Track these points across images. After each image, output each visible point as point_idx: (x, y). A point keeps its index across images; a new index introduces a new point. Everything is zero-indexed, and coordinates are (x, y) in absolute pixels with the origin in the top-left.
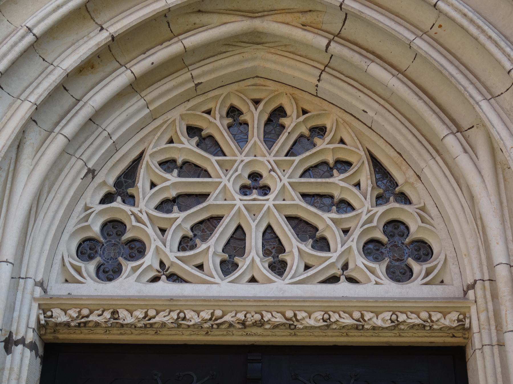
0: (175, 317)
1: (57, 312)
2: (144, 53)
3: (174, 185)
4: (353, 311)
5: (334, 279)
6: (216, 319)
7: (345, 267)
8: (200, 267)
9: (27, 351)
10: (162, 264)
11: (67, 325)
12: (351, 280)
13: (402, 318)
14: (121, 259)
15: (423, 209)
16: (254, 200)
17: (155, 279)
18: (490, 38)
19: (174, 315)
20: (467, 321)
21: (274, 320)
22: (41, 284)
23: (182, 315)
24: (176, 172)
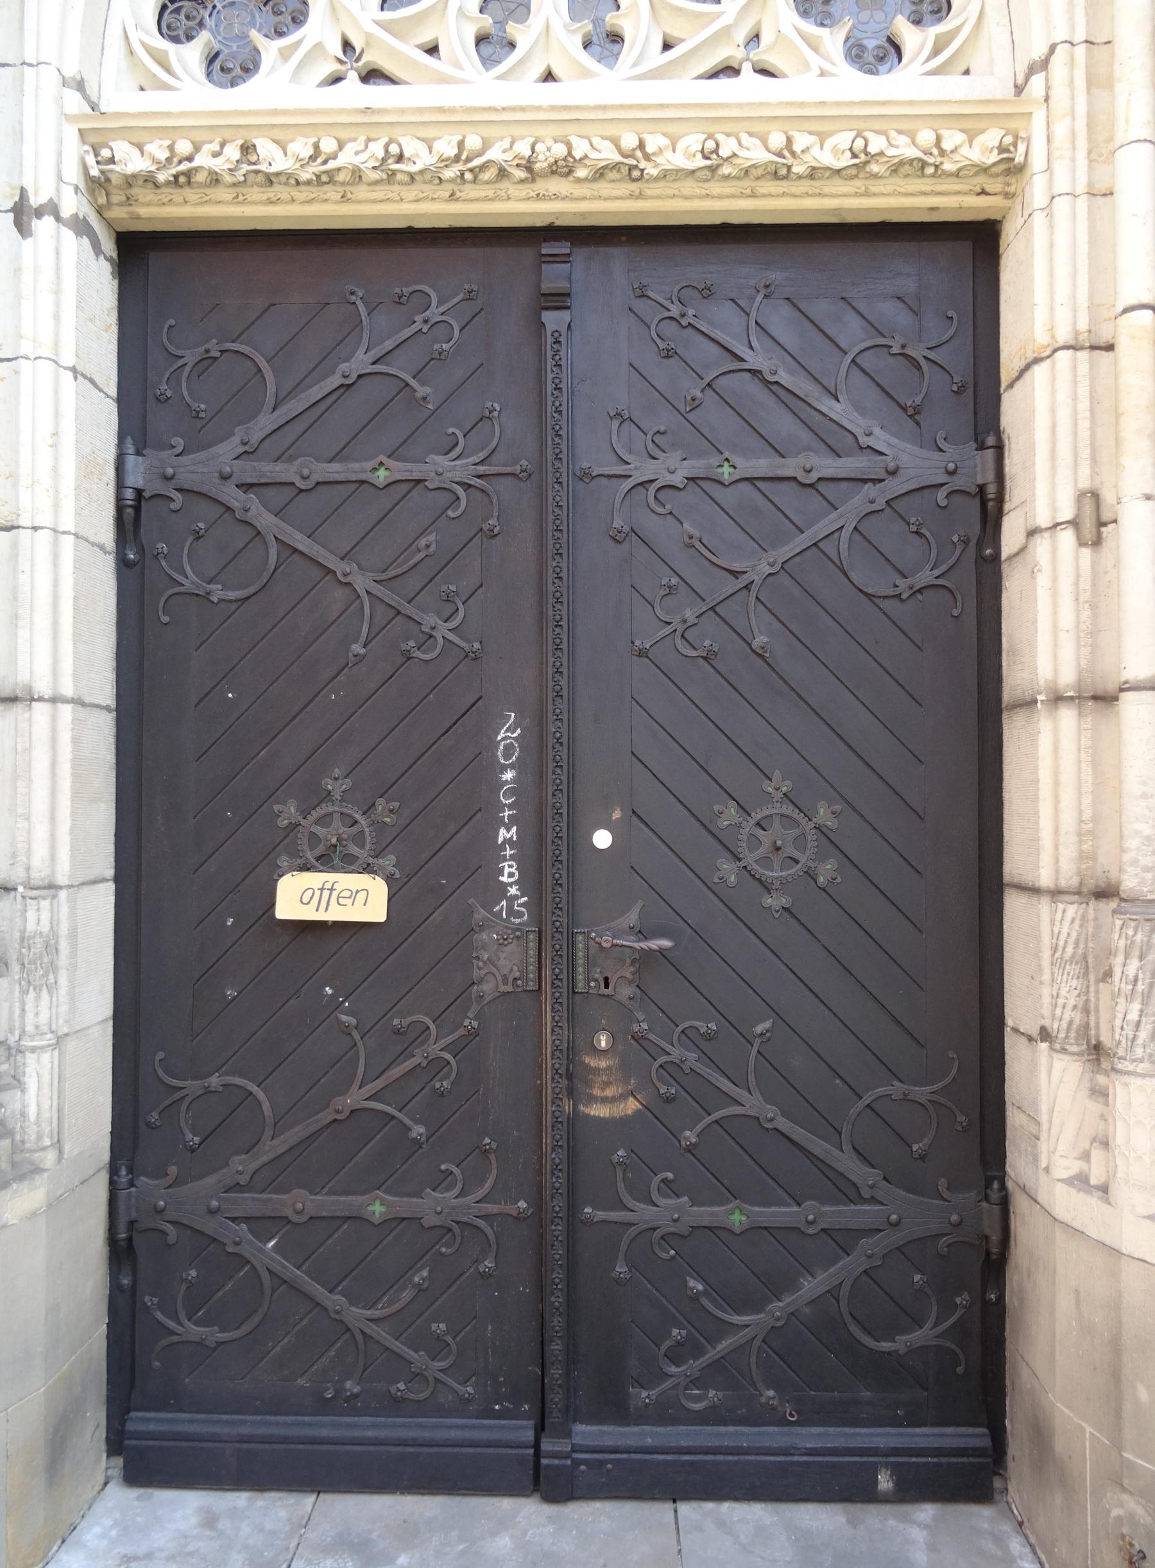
0: (381, 154)
4: (769, 132)
5: (729, 70)
6: (469, 160)
9: (68, 235)
10: (347, 45)
11: (149, 180)
13: (876, 144)
14: (255, 35)
19: (377, 149)
20: (1021, 148)
23: (394, 149)
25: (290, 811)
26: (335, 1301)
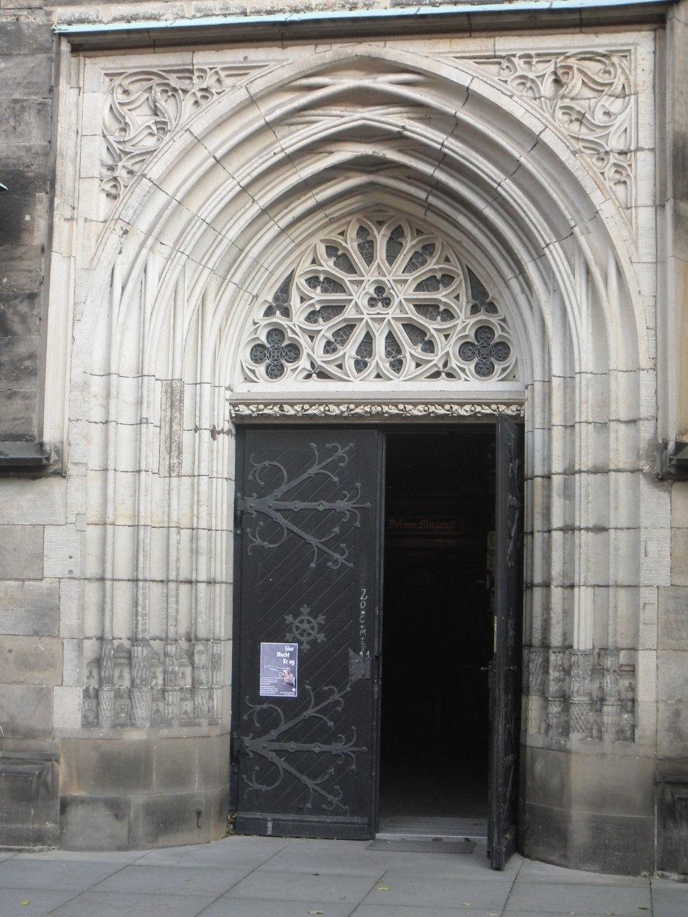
0: (323, 410)
1: (242, 407)
2: (287, 208)
3: (319, 301)
5: (436, 375)
6: (351, 410)
7: (445, 365)
8: (340, 366)
9: (226, 436)
12: (450, 375)
14: (283, 362)
15: (504, 320)
16: (379, 314)
17: (308, 376)
18: (531, 221)
20: (522, 412)
21: (390, 411)
22: (229, 388)
24: (319, 289)
25: (289, 619)
26: (304, 778)
